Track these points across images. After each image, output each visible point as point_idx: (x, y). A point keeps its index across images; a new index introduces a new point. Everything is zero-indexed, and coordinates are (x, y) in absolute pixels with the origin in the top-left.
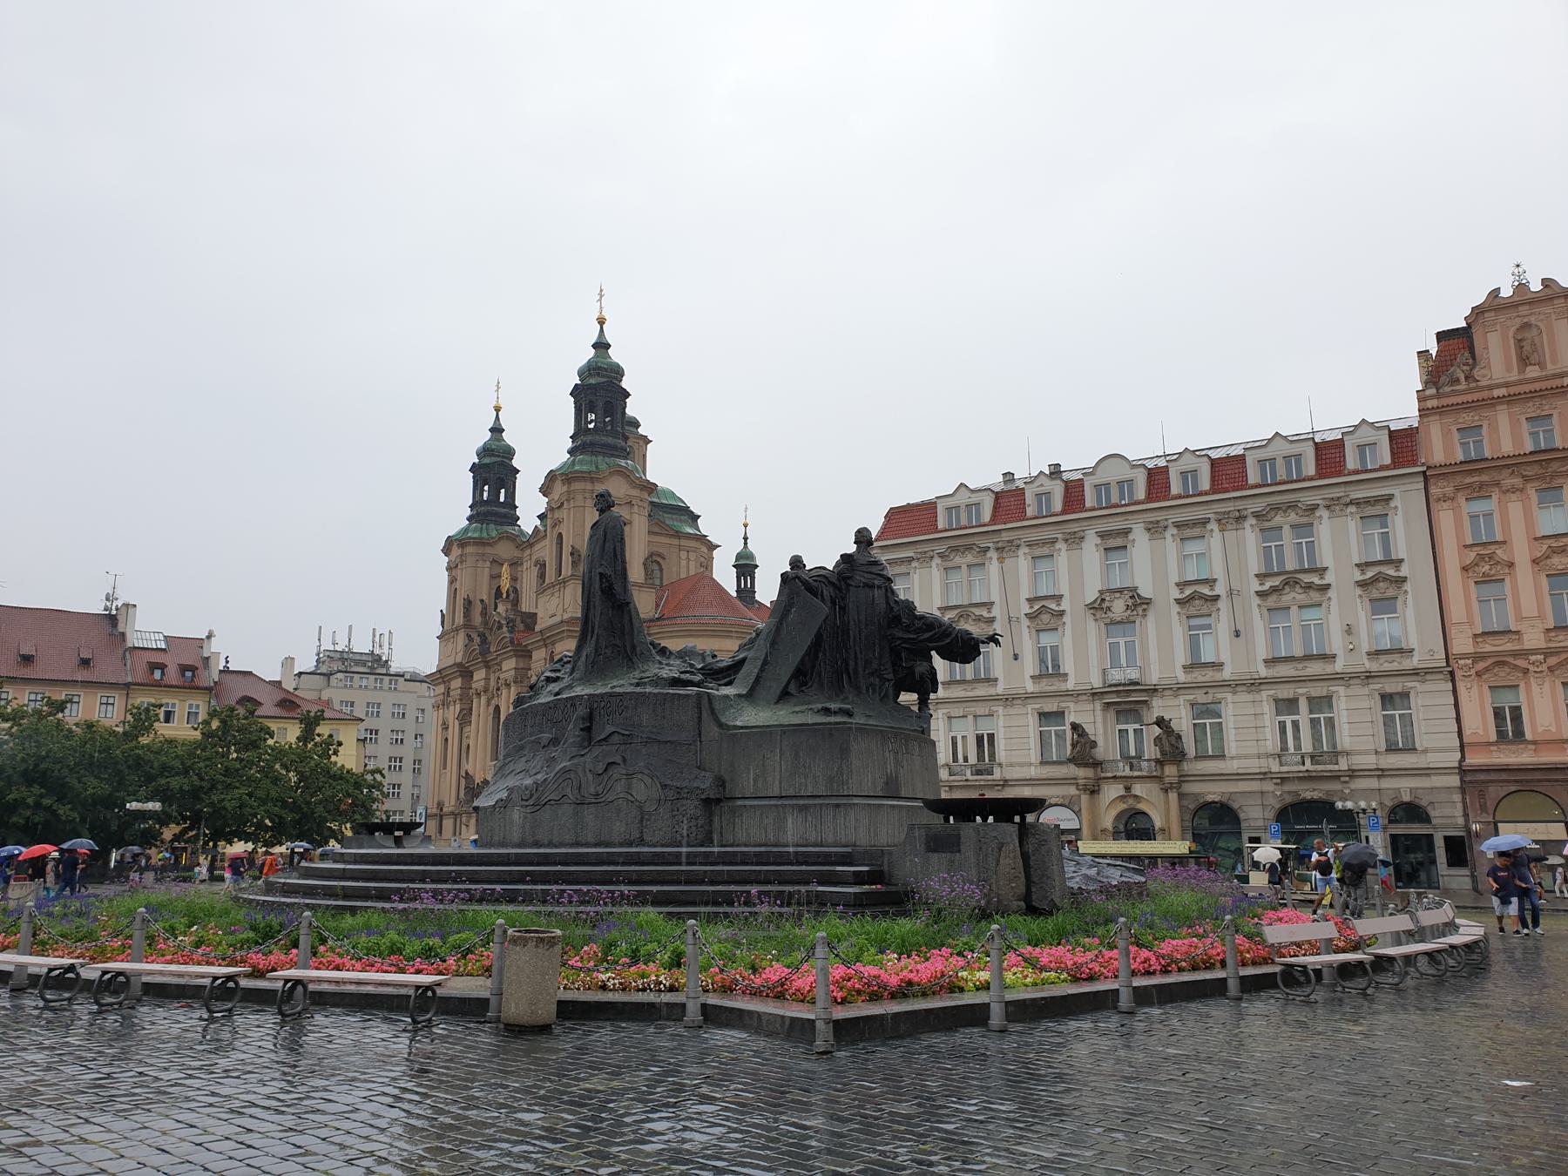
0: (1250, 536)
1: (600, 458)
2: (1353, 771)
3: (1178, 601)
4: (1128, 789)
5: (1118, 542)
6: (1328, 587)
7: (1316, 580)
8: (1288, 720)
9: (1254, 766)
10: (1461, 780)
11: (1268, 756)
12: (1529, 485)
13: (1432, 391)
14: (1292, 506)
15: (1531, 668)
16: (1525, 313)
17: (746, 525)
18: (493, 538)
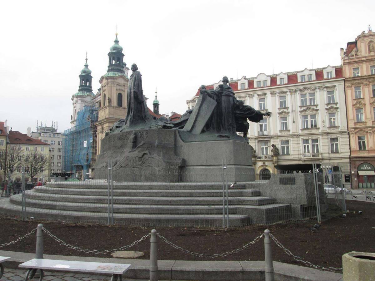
0: (298, 96)
1: (116, 72)
2: (323, 158)
3: (279, 114)
4: (264, 163)
5: (263, 97)
6: (318, 110)
7: (315, 108)
8: (306, 145)
9: (297, 157)
10: (350, 161)
11: (301, 154)
12: (370, 84)
13: (347, 58)
14: (310, 88)
15: (368, 131)
16: (372, 38)
17: (156, 93)
18: (85, 96)
